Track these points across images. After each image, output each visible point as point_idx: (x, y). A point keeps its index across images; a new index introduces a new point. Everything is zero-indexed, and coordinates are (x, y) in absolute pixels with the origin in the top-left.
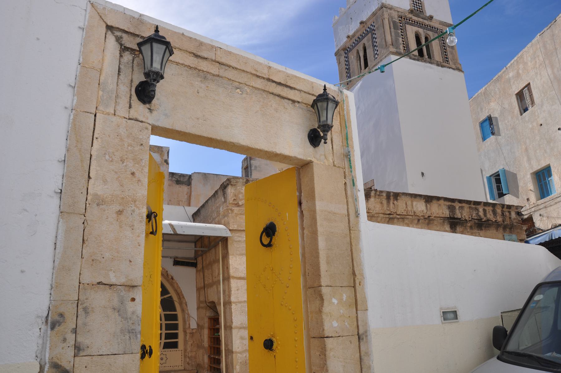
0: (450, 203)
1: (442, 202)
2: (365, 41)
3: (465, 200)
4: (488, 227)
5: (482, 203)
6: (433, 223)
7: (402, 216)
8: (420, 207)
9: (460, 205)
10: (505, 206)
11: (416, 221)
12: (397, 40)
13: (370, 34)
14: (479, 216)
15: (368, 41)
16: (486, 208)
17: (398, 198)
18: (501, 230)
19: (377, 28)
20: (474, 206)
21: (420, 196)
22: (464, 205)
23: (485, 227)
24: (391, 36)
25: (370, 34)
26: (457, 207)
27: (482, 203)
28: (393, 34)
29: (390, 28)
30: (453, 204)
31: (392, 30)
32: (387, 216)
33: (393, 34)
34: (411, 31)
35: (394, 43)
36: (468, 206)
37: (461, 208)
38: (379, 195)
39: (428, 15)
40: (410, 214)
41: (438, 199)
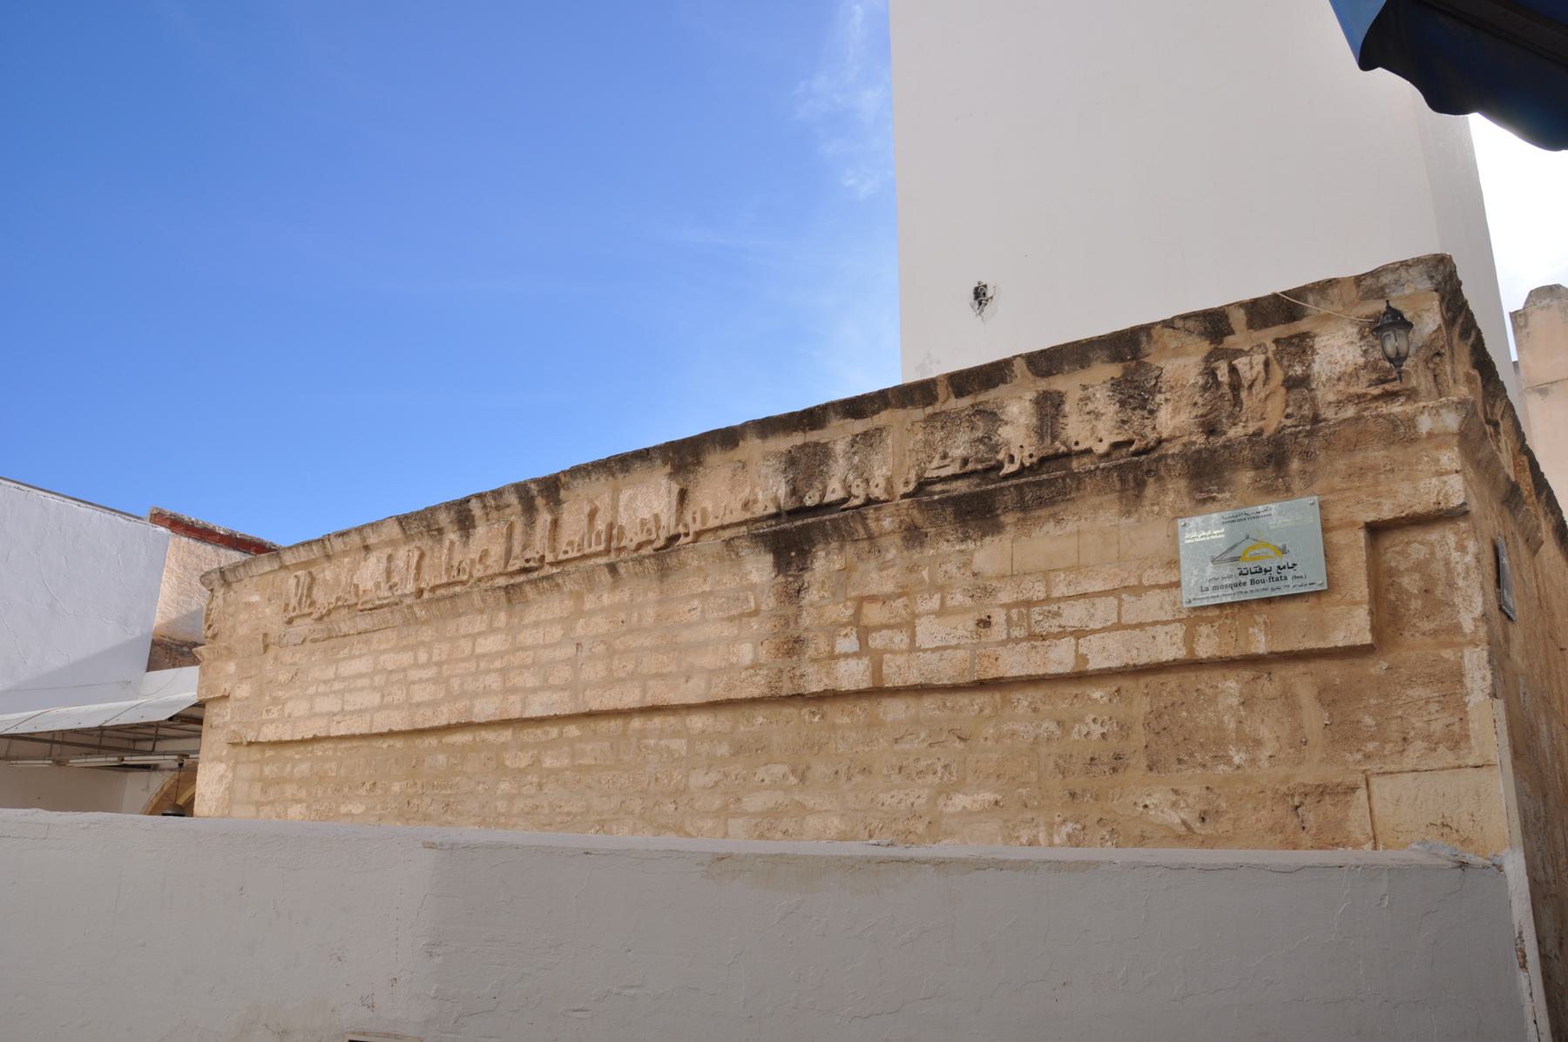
0: (798, 439)
1: (752, 447)
3: (882, 394)
4: (1041, 502)
5: (1020, 368)
6: (683, 564)
8: (648, 503)
9: (859, 426)
10: (1238, 319)
11: (606, 577)
14: (995, 449)
16: (1058, 383)
17: (563, 493)
18: (1176, 490)
20: (966, 402)
21: (643, 455)
22: (882, 418)
23: (1023, 507)
26: (840, 447)
27: (1020, 368)
30: (814, 436)
36: (918, 414)
37: (868, 439)
38: (498, 508)
40: (595, 549)
41: (728, 438)
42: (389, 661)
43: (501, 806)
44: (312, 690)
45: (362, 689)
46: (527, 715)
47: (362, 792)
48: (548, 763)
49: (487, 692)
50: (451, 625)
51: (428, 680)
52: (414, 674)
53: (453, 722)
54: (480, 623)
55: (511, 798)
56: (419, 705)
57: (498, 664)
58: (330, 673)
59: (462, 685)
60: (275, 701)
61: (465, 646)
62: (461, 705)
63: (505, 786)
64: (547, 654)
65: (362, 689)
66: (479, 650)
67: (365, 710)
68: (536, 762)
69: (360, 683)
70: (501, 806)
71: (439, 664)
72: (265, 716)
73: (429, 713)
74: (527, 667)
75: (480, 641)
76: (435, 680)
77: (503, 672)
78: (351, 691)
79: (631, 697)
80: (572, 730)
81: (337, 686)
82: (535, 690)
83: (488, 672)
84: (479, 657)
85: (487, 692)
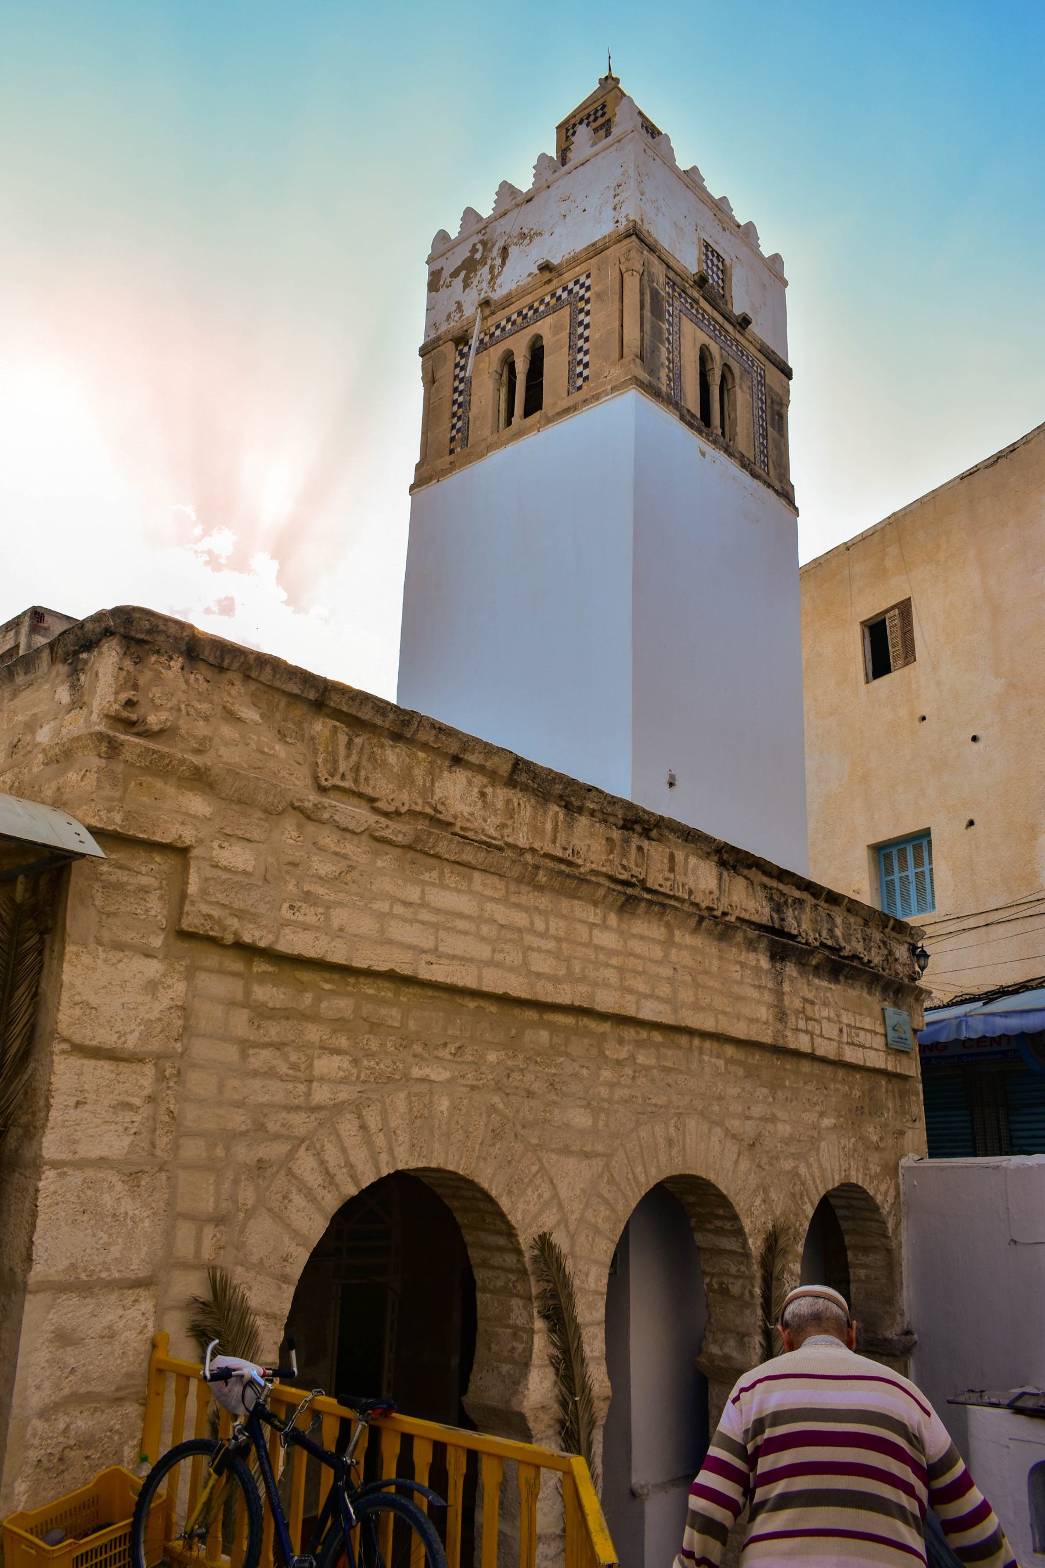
2: (544, 327)
6: (734, 936)
7: (660, 899)
12: (655, 350)
13: (566, 312)
15: (556, 329)
19: (599, 296)
24: (642, 331)
25: (566, 312)
28: (647, 327)
29: (642, 307)
31: (648, 314)
32: (619, 888)
33: (647, 327)
34: (692, 337)
35: (647, 355)
39: (737, 311)
42: (501, 913)
43: (604, 1092)
44: (383, 906)
45: (466, 933)
46: (641, 1016)
47: (445, 1053)
48: (641, 1059)
49: (606, 984)
50: (565, 905)
51: (548, 952)
52: (530, 940)
53: (577, 1004)
54: (593, 914)
55: (612, 1086)
56: (539, 975)
57: (614, 961)
58: (413, 894)
59: (583, 969)
60: (308, 897)
61: (583, 932)
62: (582, 989)
63: (606, 1074)
64: (653, 969)
65: (466, 933)
66: (595, 941)
67: (471, 960)
68: (632, 1058)
69: (461, 924)
70: (604, 1092)
71: (558, 940)
72: (286, 913)
73: (550, 987)
74: (640, 974)
75: (596, 932)
76: (557, 955)
77: (620, 970)
78: (448, 929)
79: (708, 1024)
80: (657, 1037)
81: (425, 916)
82: (646, 996)
83: (607, 966)
84: (598, 948)
85: (606, 984)
